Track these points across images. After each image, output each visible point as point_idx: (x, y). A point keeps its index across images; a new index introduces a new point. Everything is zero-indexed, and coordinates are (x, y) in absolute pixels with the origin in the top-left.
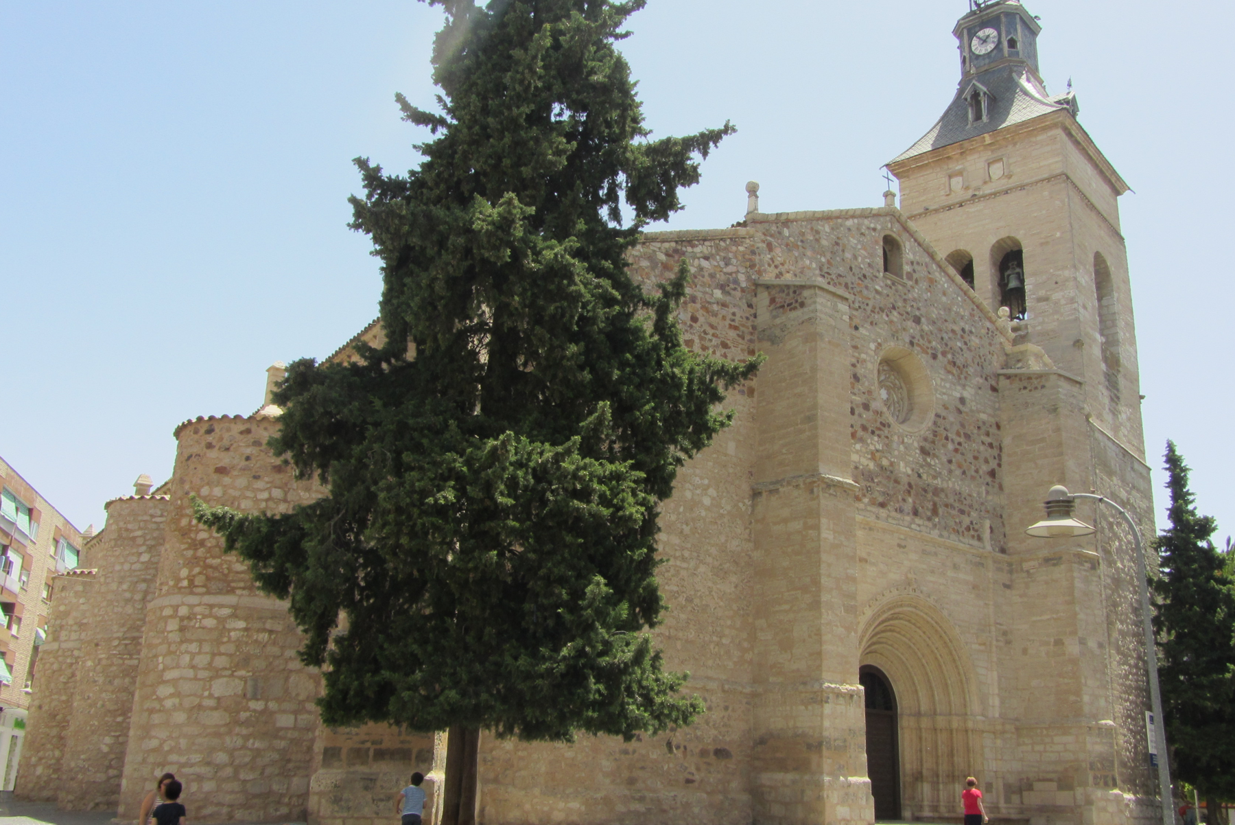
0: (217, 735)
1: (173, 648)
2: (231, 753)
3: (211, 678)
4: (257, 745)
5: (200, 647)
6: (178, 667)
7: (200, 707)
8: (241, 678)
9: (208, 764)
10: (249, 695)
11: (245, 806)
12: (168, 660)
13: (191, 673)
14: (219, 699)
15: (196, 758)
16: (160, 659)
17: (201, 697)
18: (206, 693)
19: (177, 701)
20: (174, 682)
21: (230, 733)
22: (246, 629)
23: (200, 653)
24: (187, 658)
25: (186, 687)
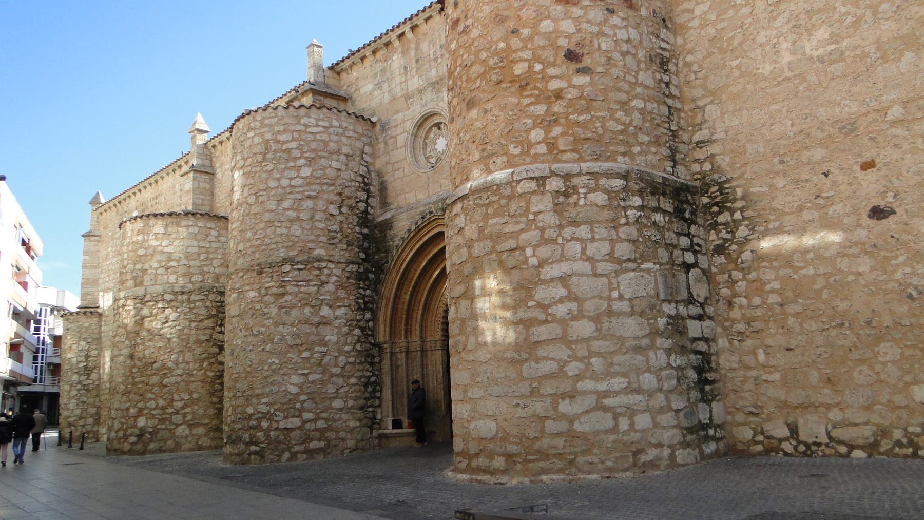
0: (639, 349)
1: (550, 233)
2: (657, 372)
3: (618, 273)
4: (678, 362)
5: (592, 230)
6: (563, 258)
7: (610, 313)
8: (648, 271)
9: (638, 391)
10: (662, 296)
11: (685, 445)
12: (545, 251)
13: (587, 267)
14: (630, 300)
15: (618, 383)
16: (529, 251)
17: (609, 298)
18: (615, 294)
19: (574, 306)
20: (563, 280)
21: (652, 346)
22: (641, 208)
23: (593, 240)
24: (578, 247)
25: (584, 286)
